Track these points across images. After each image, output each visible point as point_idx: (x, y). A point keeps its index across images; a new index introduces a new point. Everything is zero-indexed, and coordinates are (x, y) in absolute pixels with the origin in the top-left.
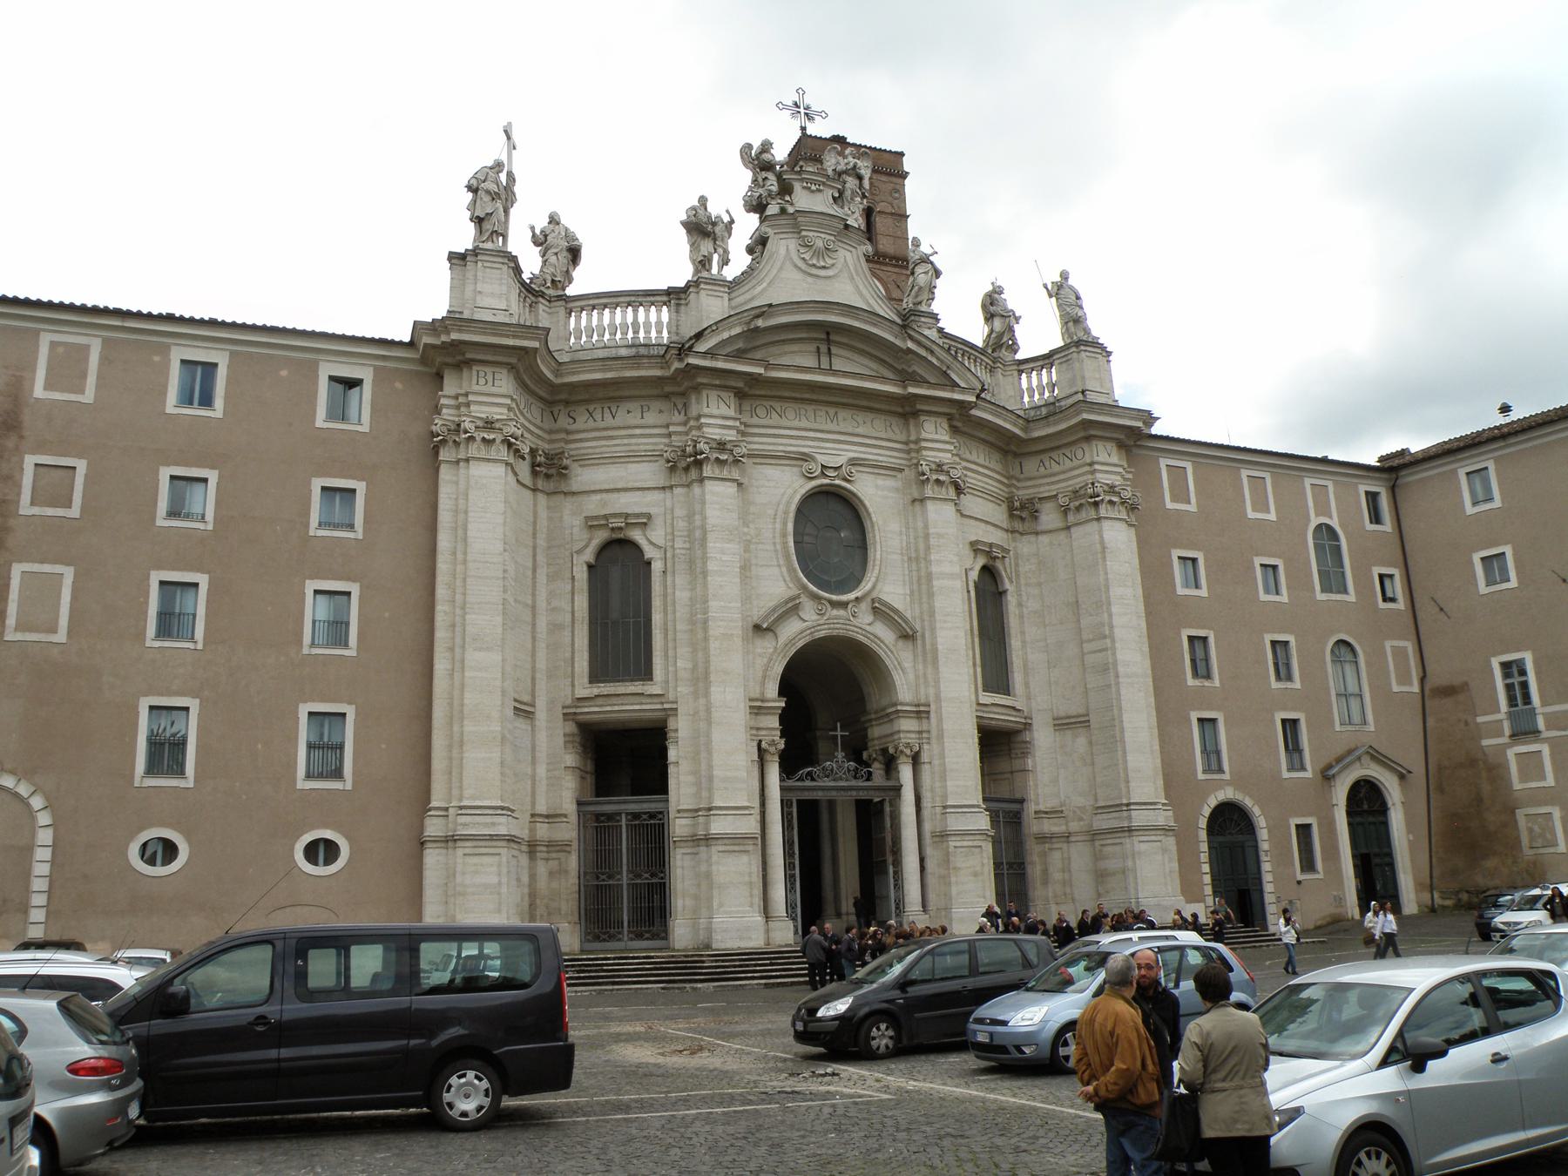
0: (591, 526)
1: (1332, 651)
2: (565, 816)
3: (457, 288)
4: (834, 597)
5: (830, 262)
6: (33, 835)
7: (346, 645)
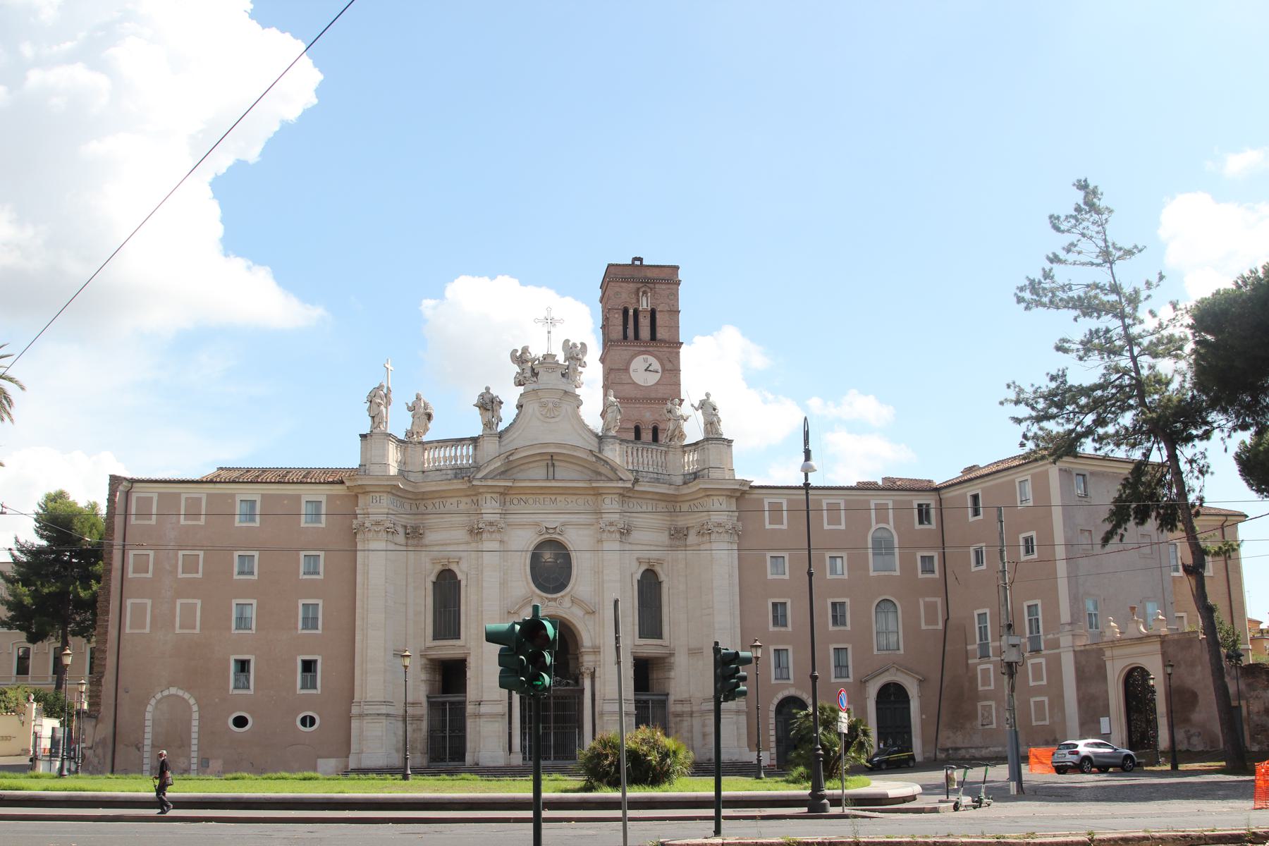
0: (434, 563)
1: (877, 605)
2: (421, 703)
3: (364, 452)
4: (549, 596)
5: (556, 413)
6: (191, 715)
7: (317, 629)
